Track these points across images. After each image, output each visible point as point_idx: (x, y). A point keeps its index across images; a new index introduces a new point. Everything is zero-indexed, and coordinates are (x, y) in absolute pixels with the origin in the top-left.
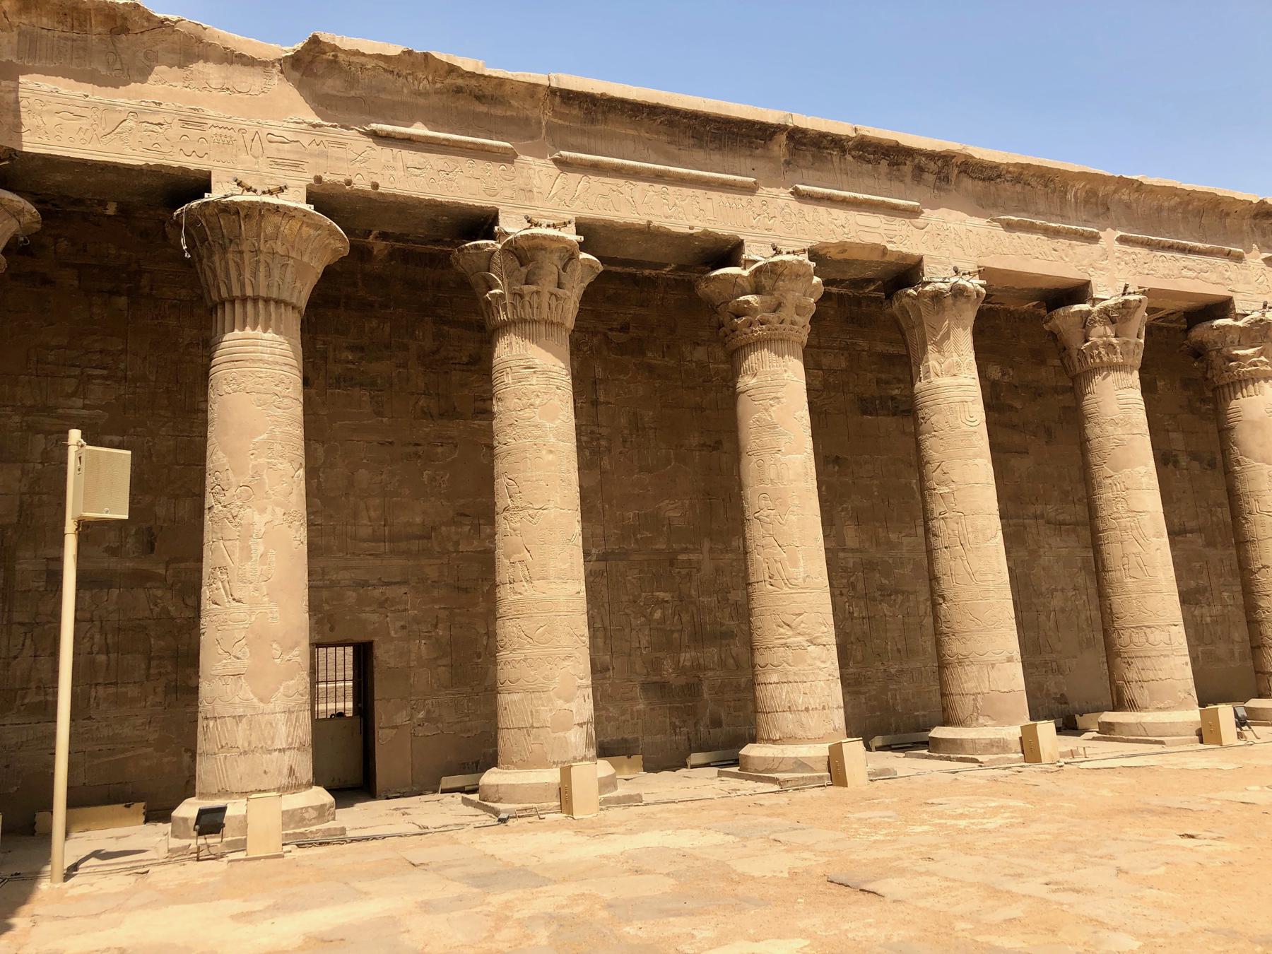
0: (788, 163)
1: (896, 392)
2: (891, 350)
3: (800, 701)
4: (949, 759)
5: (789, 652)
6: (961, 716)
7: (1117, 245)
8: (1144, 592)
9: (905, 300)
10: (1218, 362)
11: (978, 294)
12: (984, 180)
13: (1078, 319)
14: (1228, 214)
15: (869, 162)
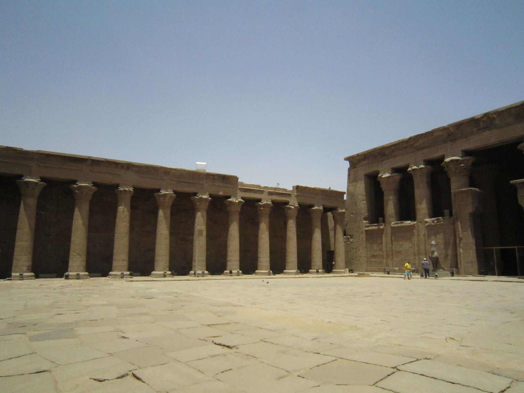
3: (74, 265)
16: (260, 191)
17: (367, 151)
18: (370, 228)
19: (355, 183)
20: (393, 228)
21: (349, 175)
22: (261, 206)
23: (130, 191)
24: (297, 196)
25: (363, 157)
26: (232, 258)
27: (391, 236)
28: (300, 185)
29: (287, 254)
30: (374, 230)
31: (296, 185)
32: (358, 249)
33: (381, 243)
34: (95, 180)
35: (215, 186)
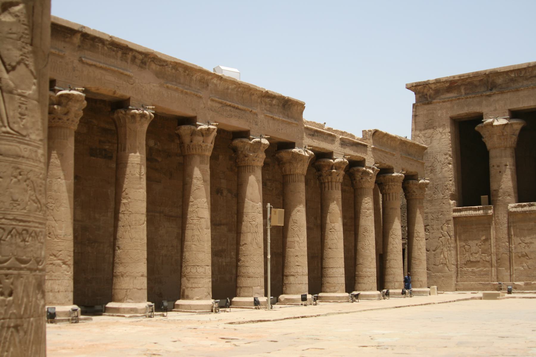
0: (79, 46)
1: (107, 147)
2: (107, 126)
3: (56, 287)
4: (113, 316)
5: (54, 267)
6: (120, 298)
7: (210, 103)
8: (199, 251)
9: (120, 115)
10: (241, 156)
11: (151, 116)
12: (160, 65)
13: (189, 132)
14: (253, 94)
15: (114, 51)
16: (329, 136)
17: (460, 76)
18: (463, 213)
19: (430, 131)
20: (510, 214)
21: (415, 116)
22: (332, 167)
23: (151, 116)
24: (373, 149)
25: (448, 84)
26: (299, 270)
27: (509, 228)
28: (380, 129)
29: (361, 261)
30: (471, 217)
31: (372, 128)
32: (438, 251)
33: (487, 239)
34: (88, 86)
35: (274, 119)
